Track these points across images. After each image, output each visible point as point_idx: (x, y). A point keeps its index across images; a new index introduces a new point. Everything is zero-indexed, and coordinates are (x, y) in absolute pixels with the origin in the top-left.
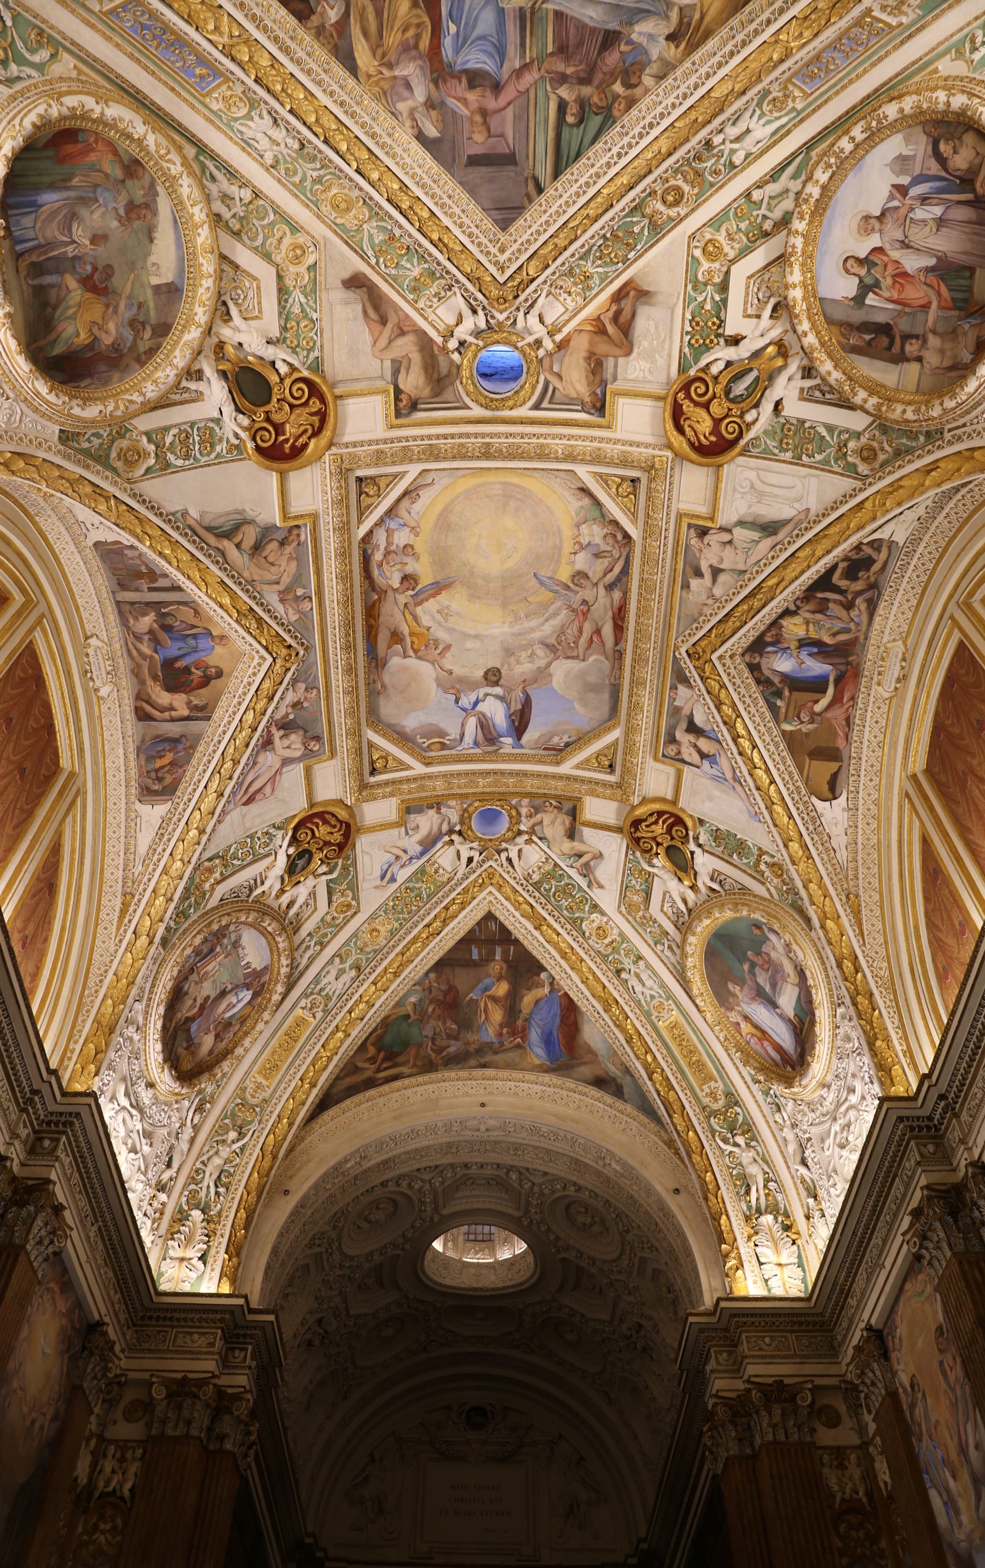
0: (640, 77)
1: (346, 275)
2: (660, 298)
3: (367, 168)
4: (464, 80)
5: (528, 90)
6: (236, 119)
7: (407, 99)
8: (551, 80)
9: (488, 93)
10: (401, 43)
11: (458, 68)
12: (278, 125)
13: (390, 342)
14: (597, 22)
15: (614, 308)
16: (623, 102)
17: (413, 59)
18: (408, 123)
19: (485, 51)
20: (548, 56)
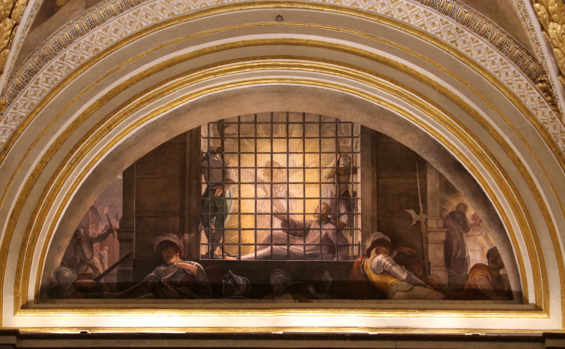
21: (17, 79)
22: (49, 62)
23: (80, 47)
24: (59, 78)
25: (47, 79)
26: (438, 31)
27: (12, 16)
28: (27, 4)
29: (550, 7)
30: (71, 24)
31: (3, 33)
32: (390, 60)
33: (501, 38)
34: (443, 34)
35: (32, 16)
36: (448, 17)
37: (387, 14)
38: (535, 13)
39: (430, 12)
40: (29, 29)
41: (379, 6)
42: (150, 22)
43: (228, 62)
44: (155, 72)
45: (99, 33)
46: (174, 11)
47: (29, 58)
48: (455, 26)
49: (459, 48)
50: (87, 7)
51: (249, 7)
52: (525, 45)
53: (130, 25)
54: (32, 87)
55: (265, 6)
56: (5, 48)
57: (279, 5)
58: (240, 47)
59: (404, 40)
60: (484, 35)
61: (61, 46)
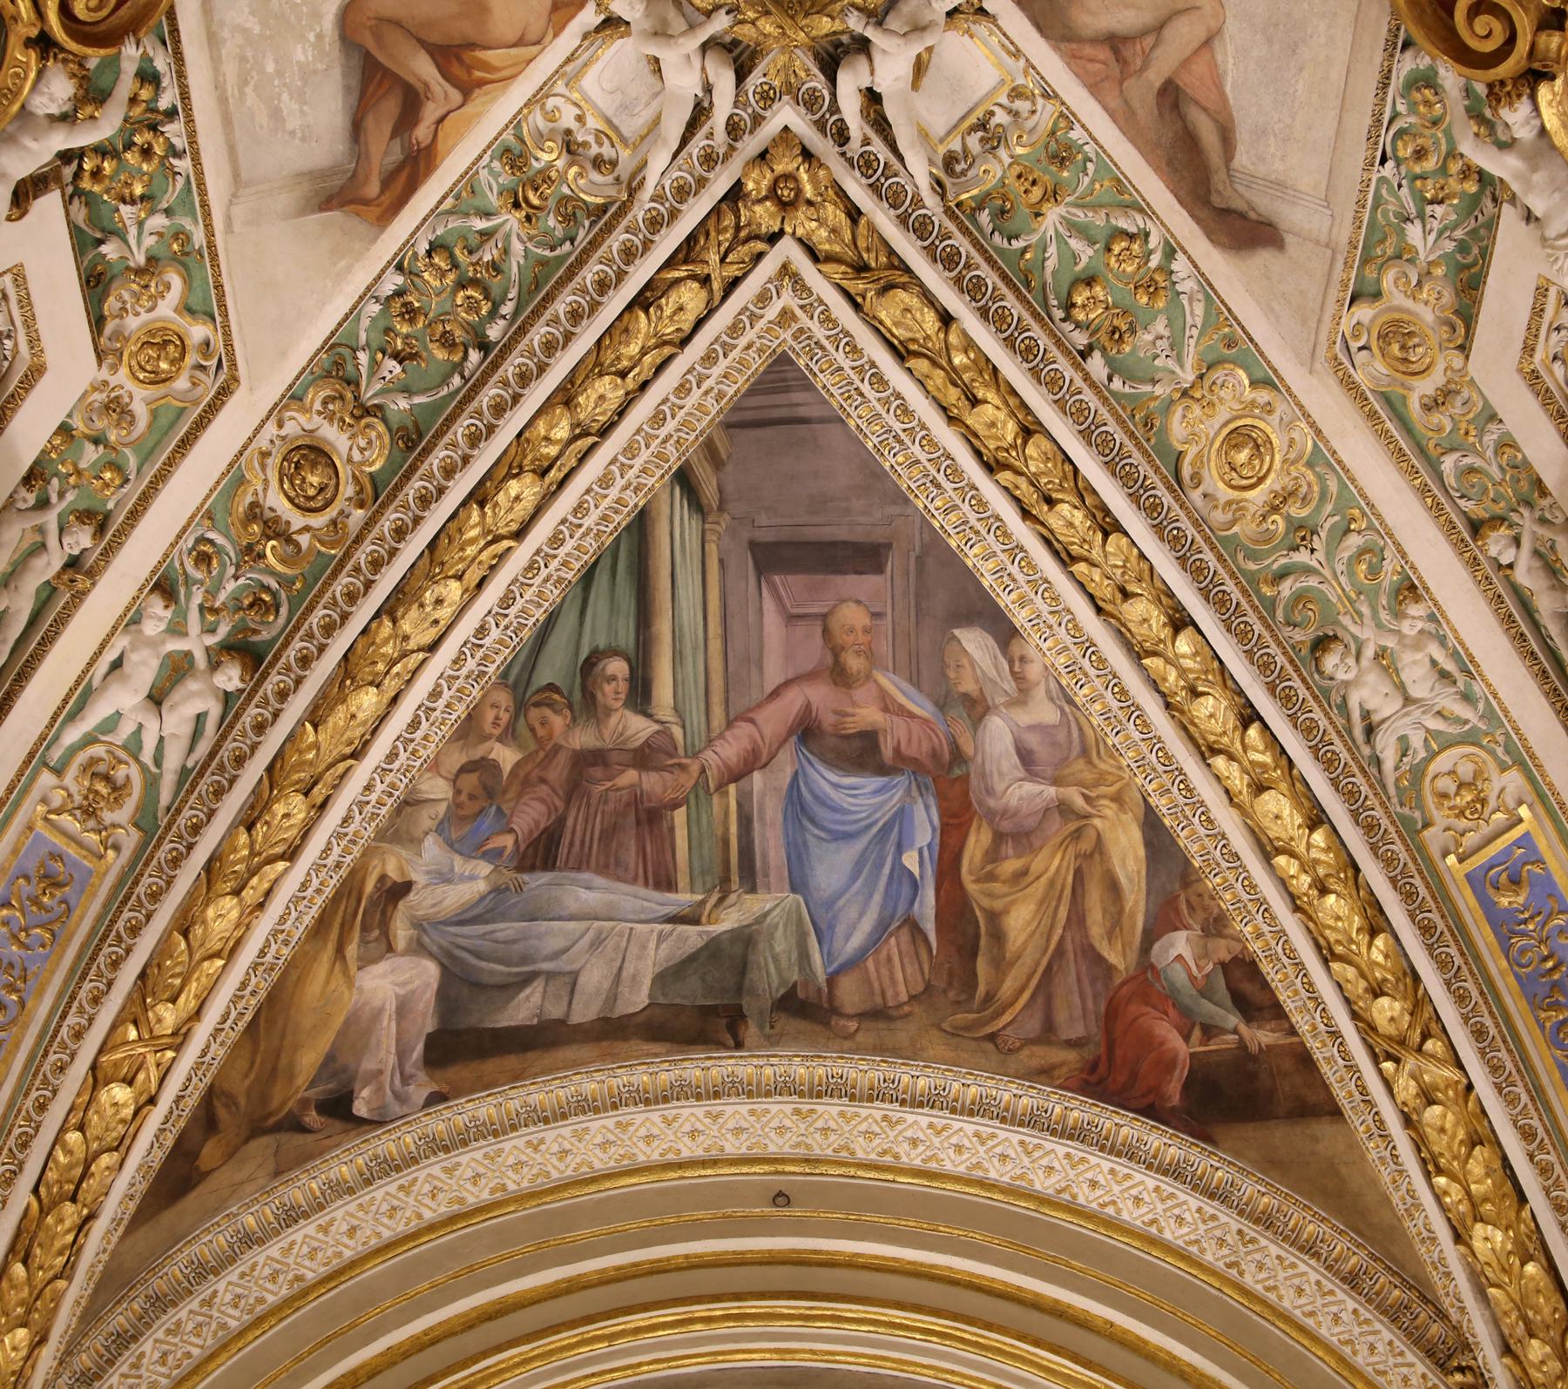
0: (458, 792)
1: (1264, 258)
2: (285, 200)
3: (1157, 621)
4: (887, 752)
5: (730, 724)
6: (1470, 738)
7: (1032, 728)
8: (671, 751)
9: (828, 720)
10: (1034, 851)
11: (901, 780)
12: (1366, 715)
13: (1159, 28)
14: (574, 882)
15: (422, 133)
16: (488, 728)
17: (1005, 813)
18: (1034, 671)
19: (836, 809)
20: (686, 801)
21: (84, 1356)
22: (171, 1311)
23: (256, 1273)
24: (196, 1351)
25: (165, 1354)
26: (1193, 1237)
27: (80, 1197)
28: (121, 1166)
29: (1473, 1187)
30: (235, 1215)
31: (53, 1239)
32: (1069, 1306)
33: (1354, 1260)
34: (1205, 1245)
35: (132, 1197)
36: (1215, 1203)
37: (1059, 1192)
38: (1438, 1199)
39: (1171, 1190)
40: (121, 1229)
41: (1040, 1173)
42: (443, 1209)
43: (645, 1308)
44: (452, 1334)
45: (306, 1236)
46: (506, 1181)
47: (119, 1302)
48: (1235, 1226)
49: (1248, 1280)
50: (277, 1173)
51: (703, 1172)
52: (1414, 1277)
53: (391, 1217)
54: (122, 1375)
55: (745, 1169)
56: (56, 1277)
57: (780, 1168)
58: (678, 1269)
59: (1105, 1257)
60: (1309, 1249)
61: (204, 1271)
